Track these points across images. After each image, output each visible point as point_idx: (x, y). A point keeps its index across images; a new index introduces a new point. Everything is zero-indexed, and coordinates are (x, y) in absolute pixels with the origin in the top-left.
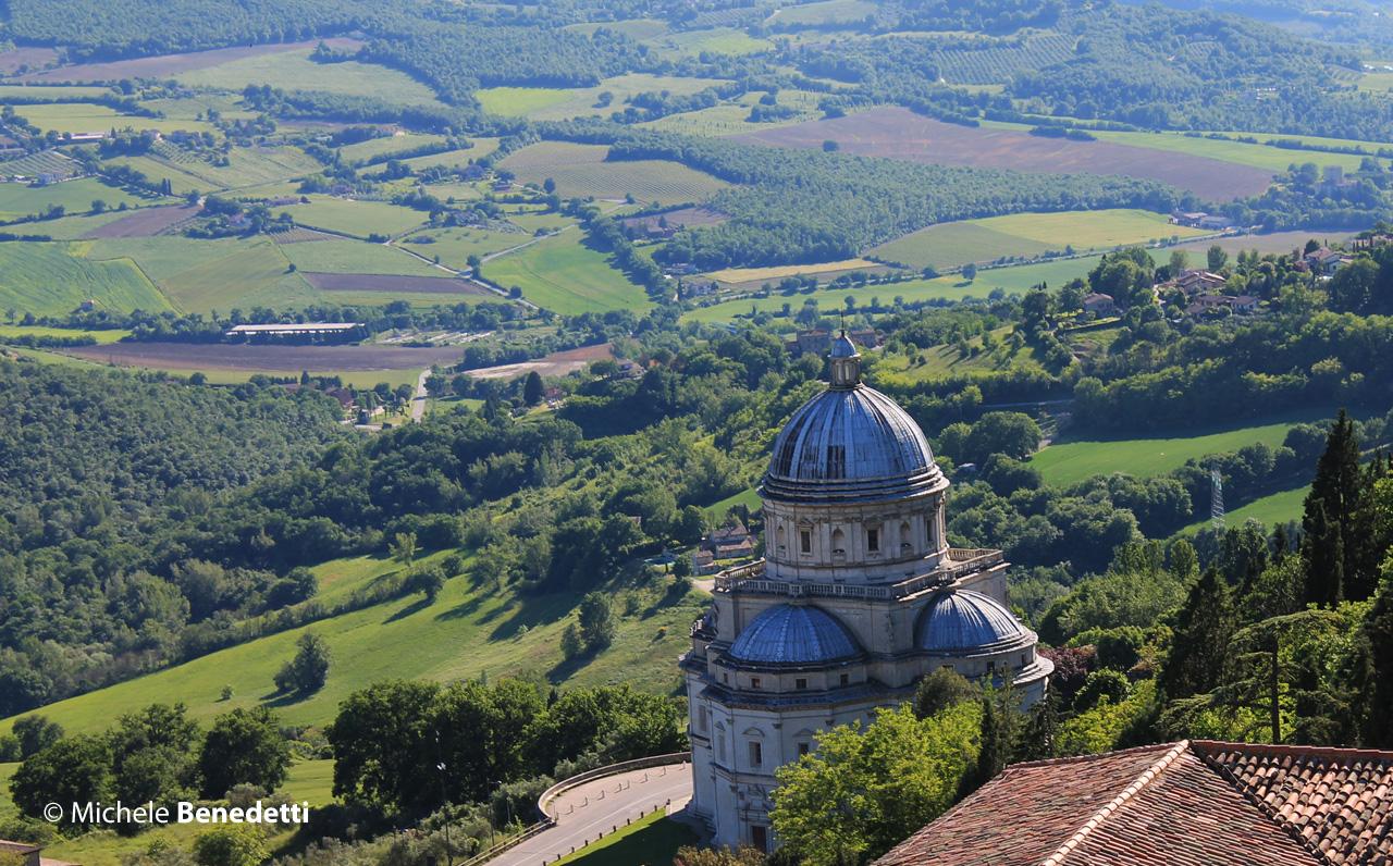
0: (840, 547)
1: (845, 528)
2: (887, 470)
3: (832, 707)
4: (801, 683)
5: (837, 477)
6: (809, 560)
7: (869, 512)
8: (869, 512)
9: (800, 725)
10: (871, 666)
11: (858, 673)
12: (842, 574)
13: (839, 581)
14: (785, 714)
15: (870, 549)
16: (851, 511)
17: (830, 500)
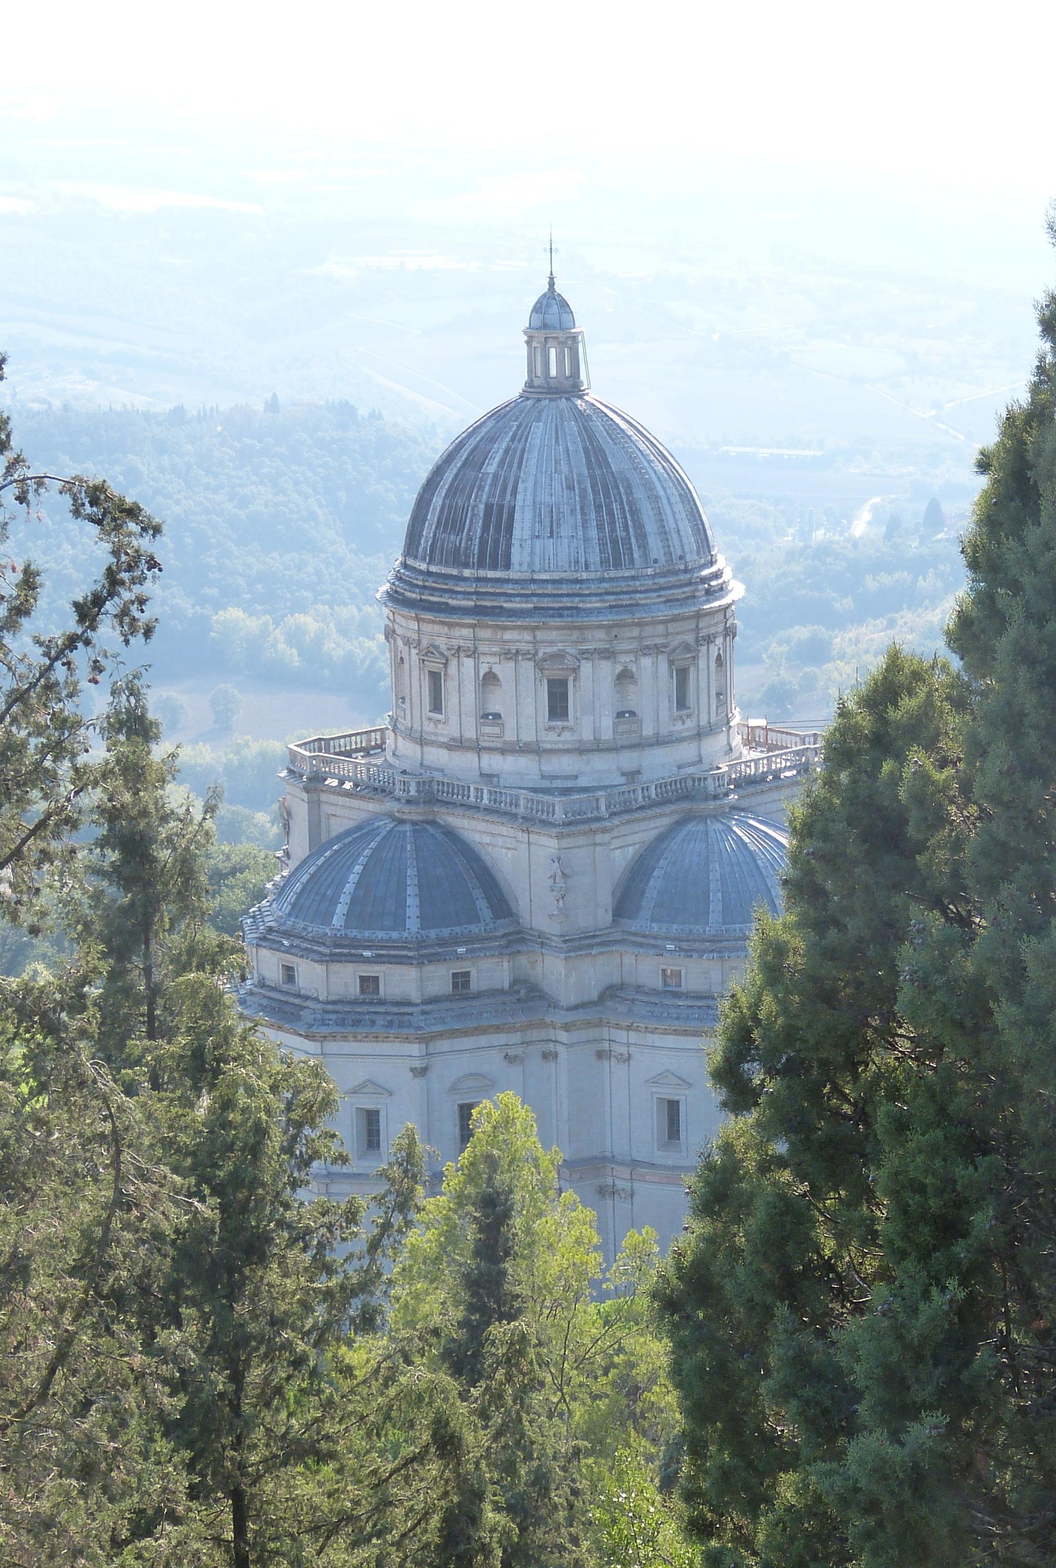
0: (495, 707)
1: (504, 670)
2: (595, 558)
3: (425, 1040)
4: (369, 983)
5: (494, 567)
6: (441, 729)
7: (551, 643)
8: (551, 643)
9: (359, 1072)
10: (522, 960)
11: (491, 972)
12: (493, 762)
13: (488, 777)
14: (331, 1047)
15: (550, 719)
16: (517, 638)
17: (478, 611)
